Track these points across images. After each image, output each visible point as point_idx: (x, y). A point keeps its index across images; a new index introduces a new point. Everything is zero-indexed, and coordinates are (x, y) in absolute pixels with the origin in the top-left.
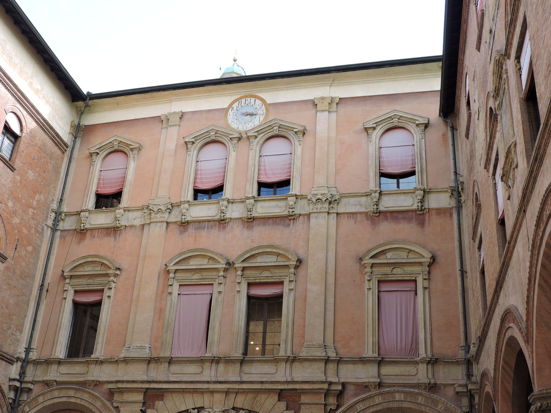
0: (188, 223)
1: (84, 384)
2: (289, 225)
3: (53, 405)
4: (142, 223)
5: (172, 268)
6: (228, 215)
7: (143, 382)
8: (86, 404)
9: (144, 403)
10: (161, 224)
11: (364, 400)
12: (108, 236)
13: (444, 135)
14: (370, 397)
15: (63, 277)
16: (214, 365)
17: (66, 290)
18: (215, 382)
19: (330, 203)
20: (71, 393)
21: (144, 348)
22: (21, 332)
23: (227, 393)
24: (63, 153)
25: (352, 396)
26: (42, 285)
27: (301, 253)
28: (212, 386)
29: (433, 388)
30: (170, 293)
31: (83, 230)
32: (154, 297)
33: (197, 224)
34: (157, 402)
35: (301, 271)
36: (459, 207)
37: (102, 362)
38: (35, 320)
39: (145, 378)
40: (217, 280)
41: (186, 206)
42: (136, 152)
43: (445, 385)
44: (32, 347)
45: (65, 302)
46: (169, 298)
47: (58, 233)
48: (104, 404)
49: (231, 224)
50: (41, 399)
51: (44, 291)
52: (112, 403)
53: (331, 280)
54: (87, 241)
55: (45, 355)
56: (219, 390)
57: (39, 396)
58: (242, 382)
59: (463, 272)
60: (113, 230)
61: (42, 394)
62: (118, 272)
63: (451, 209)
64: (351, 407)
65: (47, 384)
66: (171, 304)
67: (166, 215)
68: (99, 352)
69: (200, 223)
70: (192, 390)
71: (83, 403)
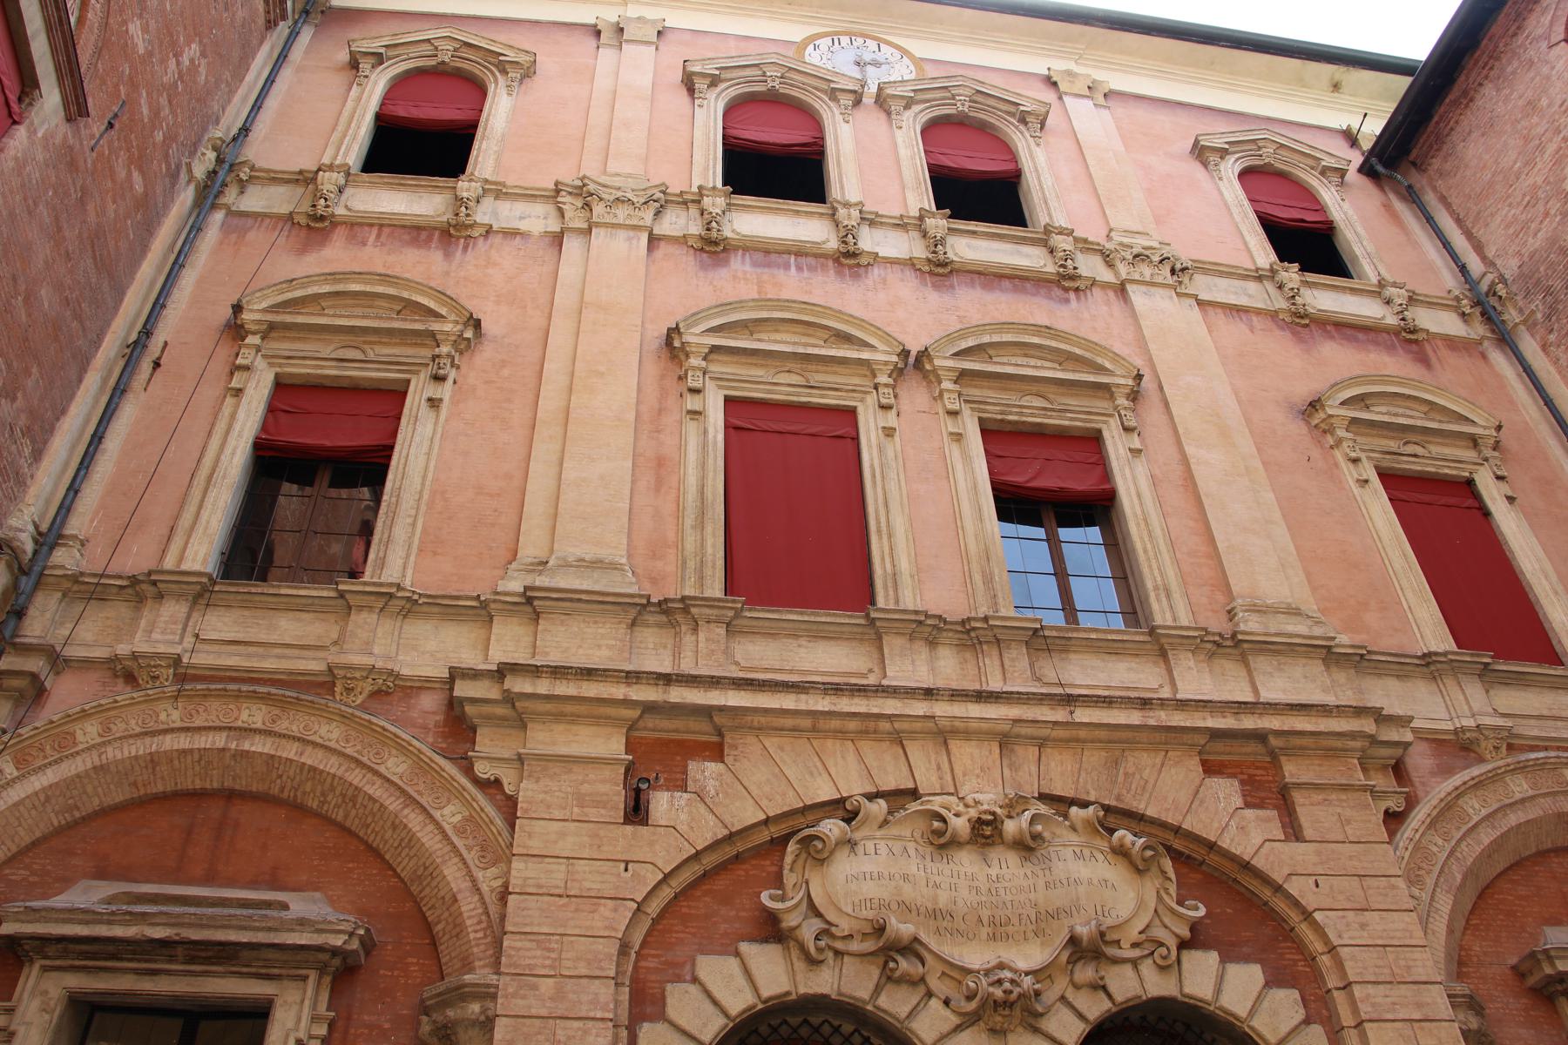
2: (1067, 301)
3: (153, 760)
4: (555, 226)
5: (696, 337)
8: (332, 765)
10: (631, 233)
12: (419, 247)
13: (1387, 207)
15: (235, 330)
17: (247, 368)
18: (957, 695)
19: (1173, 272)
20: (253, 715)
21: (614, 567)
22: (37, 455)
23: (1006, 741)
24: (271, 24)
25: (1433, 774)
26: (147, 333)
27: (1139, 362)
28: (942, 709)
30: (695, 414)
31: (322, 218)
32: (631, 416)
33: (759, 256)
34: (692, 766)
35: (1152, 415)
36: (1505, 340)
38: (97, 438)
40: (871, 399)
44: (67, 531)
45: (237, 406)
46: (692, 428)
47: (218, 216)
49: (876, 271)
51: (146, 366)
52: (468, 770)
53: (1246, 445)
55: (136, 559)
56: (974, 725)
57: (84, 715)
61: (100, 710)
64: (1448, 807)
65: (126, 672)
66: (704, 446)
67: (648, 216)
69: (768, 252)
70: (852, 725)
71: (311, 758)
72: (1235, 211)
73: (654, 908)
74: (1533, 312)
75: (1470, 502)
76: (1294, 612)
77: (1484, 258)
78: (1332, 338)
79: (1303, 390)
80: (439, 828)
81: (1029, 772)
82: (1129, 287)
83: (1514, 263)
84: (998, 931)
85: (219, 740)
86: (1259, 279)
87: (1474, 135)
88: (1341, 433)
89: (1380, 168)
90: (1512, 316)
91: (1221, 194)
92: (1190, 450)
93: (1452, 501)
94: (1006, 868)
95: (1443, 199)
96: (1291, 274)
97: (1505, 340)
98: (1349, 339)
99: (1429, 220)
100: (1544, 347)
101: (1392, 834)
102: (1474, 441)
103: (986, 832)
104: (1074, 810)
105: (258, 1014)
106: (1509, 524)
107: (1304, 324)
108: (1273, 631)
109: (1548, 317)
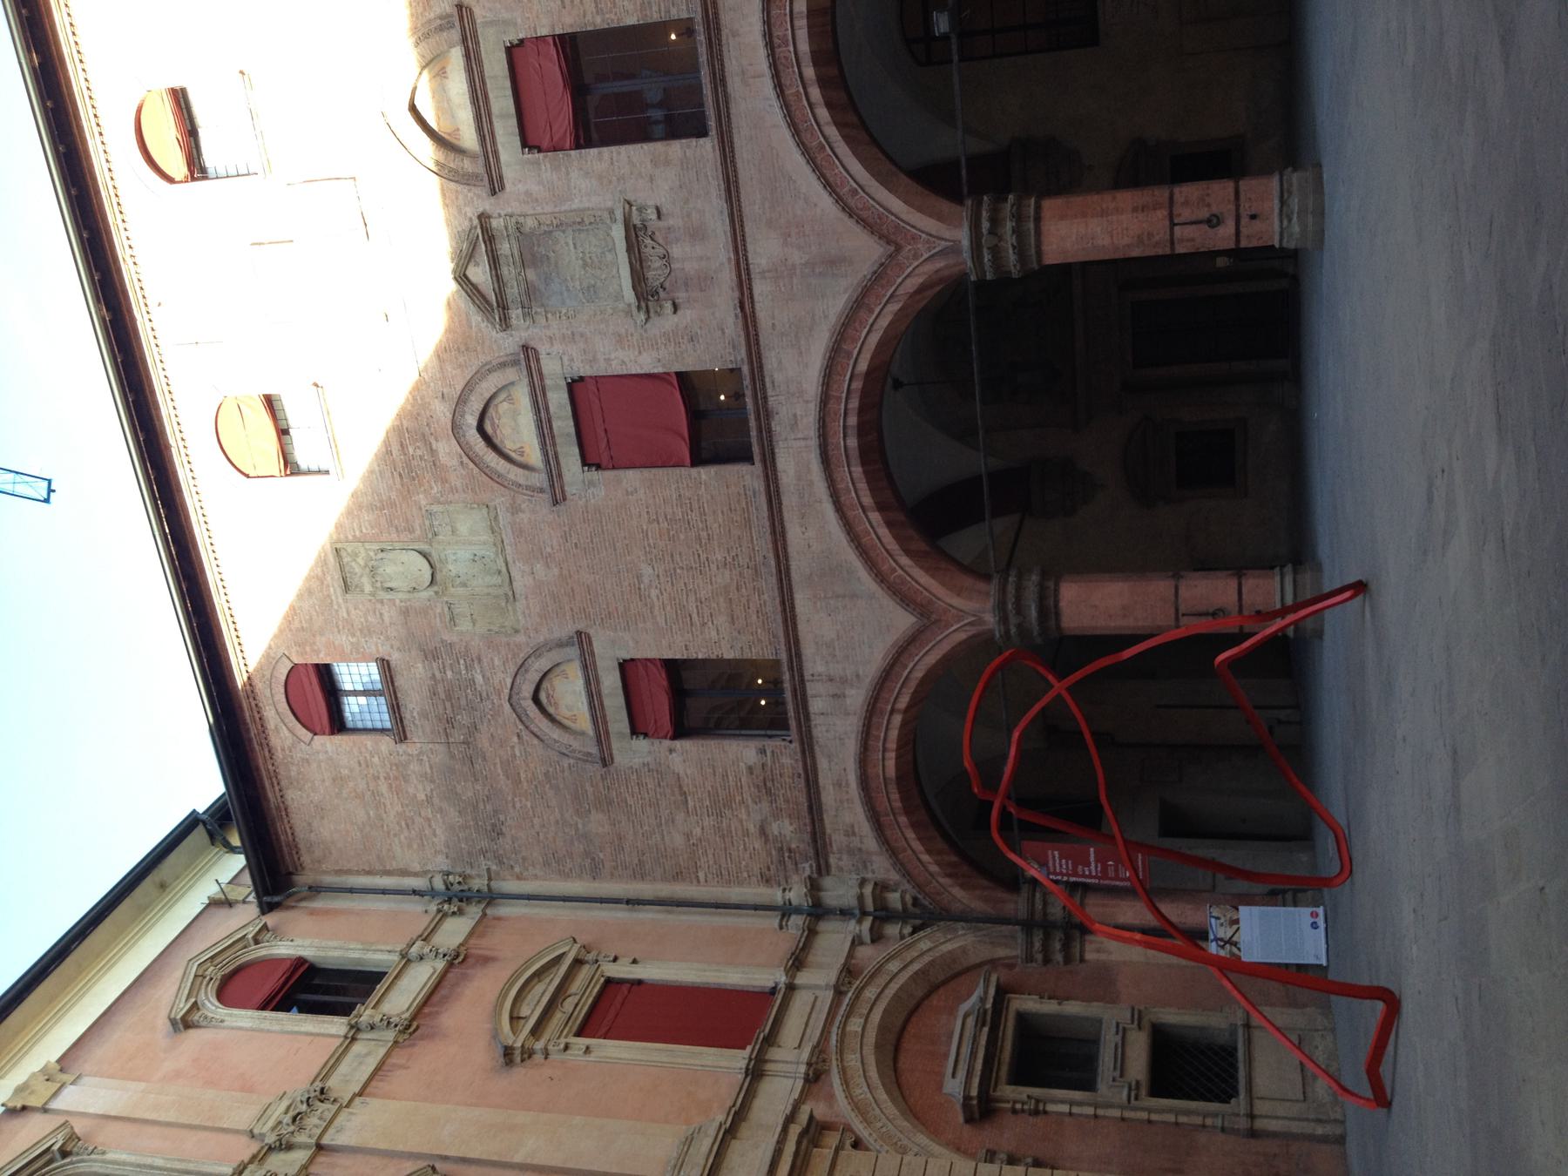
11: (846, 1082)
13: (313, 912)
14: (843, 1071)
25: (831, 1106)
29: (849, 970)
36: (491, 898)
43: (850, 955)
59: (633, 902)
63: (484, 915)
72: (266, 1025)
74: (488, 870)
75: (625, 988)
76: (689, 1141)
77: (416, 875)
78: (437, 1013)
79: (482, 1054)
82: (325, 1141)
83: (440, 859)
86: (354, 1039)
87: (315, 824)
88: (539, 1045)
89: (276, 899)
90: (478, 883)
91: (240, 1028)
92: (518, 1159)
93: (619, 999)
95: (339, 872)
96: (366, 1014)
97: (491, 898)
98: (445, 999)
99: (351, 890)
100: (519, 877)
101: (867, 1149)
102: (578, 962)
106: (650, 972)
107: (414, 1027)
108: (702, 1162)
109: (501, 863)
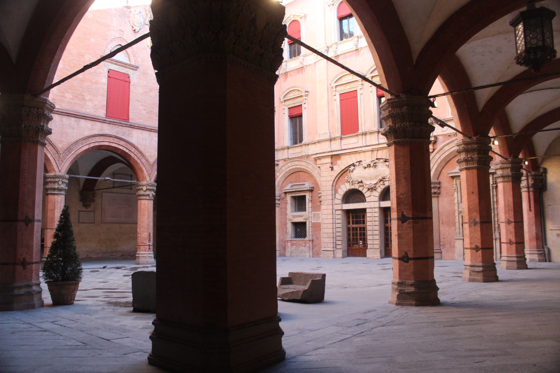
0: (338, 56)
1: (302, 157)
3: (290, 170)
6: (359, 47)
7: (328, 152)
8: (305, 168)
9: (332, 163)
11: (448, 144)
16: (364, 136)
18: (365, 146)
20: (297, 163)
37: (308, 144)
39: (329, 150)
41: (335, 46)
42: (303, 19)
48: (313, 166)
49: (362, 51)
50: (283, 168)
54: (289, 79)
58: (379, 144)
60: (301, 69)
62: (307, 93)
68: (305, 140)
73: (336, 180)
80: (315, 173)
81: (375, 155)
84: (371, 179)
85: (294, 167)
94: (372, 170)
103: (369, 166)
104: (382, 160)
105: (305, 196)
